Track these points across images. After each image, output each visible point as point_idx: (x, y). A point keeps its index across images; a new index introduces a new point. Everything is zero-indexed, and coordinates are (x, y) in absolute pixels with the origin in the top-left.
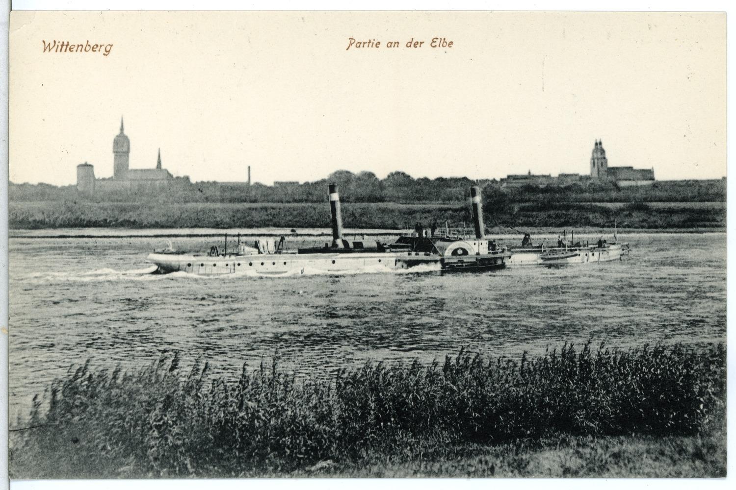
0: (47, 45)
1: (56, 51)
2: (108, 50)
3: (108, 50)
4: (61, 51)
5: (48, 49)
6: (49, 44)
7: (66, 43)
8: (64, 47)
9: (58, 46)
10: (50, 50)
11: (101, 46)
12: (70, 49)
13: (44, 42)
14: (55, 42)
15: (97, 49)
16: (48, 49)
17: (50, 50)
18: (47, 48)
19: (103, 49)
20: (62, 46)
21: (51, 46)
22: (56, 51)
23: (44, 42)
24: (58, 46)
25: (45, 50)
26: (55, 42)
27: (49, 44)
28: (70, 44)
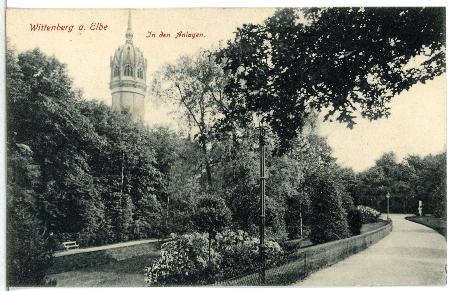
0: (33, 26)
1: (39, 30)
2: (70, 29)
3: (70, 29)
4: (42, 30)
5: (33, 29)
6: (34, 26)
7: (44, 25)
8: (44, 28)
9: (40, 27)
10: (34, 30)
11: (67, 27)
12: (47, 29)
13: (31, 25)
14: (38, 24)
15: (64, 29)
16: (33, 29)
17: (34, 30)
18: (33, 28)
19: (68, 28)
20: (43, 27)
21: (36, 27)
22: (39, 30)
23: (31, 25)
24: (40, 27)
25: (32, 29)
26: (38, 24)
27: (34, 26)
28: (47, 26)
